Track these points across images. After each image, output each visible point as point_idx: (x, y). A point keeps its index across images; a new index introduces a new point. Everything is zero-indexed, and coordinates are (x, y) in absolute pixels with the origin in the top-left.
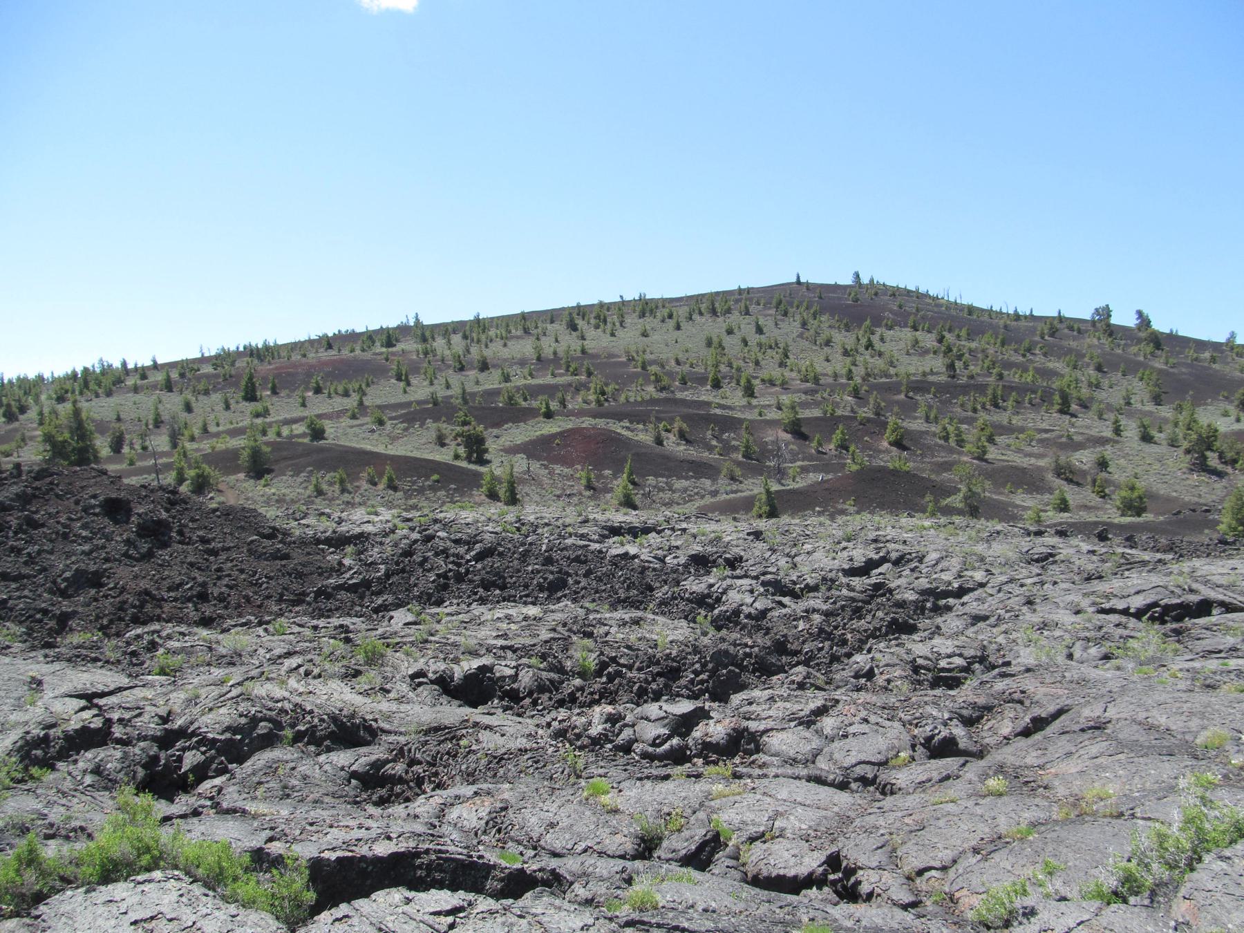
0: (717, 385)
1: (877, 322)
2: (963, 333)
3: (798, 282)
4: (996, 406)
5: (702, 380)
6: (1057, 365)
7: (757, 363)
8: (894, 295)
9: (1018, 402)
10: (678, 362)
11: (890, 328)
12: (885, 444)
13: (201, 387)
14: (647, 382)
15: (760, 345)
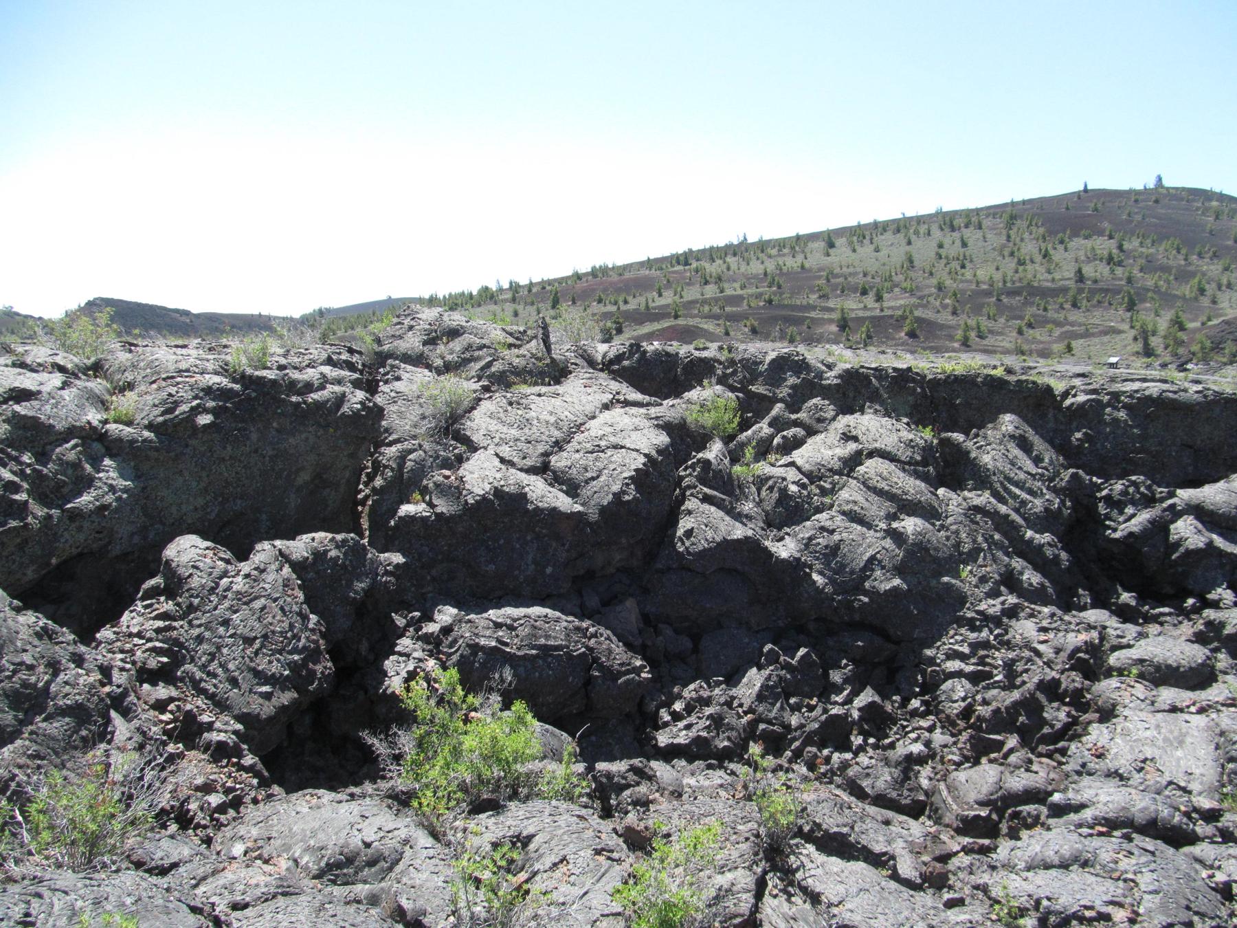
0: (864, 292)
1: (1075, 234)
2: (1149, 242)
3: (1086, 190)
4: (1075, 305)
5: (854, 289)
6: (1212, 267)
7: (931, 274)
8: (1157, 201)
9: (1099, 302)
10: (865, 275)
11: (1086, 238)
12: (903, 334)
13: (529, 300)
14: (813, 292)
15: (947, 257)
